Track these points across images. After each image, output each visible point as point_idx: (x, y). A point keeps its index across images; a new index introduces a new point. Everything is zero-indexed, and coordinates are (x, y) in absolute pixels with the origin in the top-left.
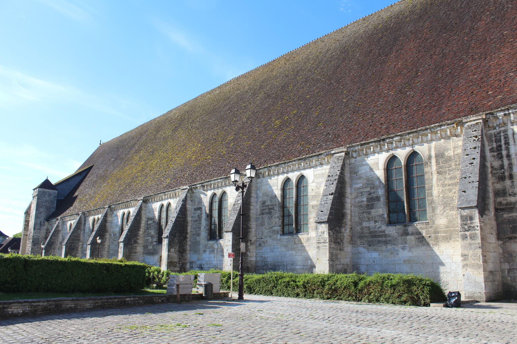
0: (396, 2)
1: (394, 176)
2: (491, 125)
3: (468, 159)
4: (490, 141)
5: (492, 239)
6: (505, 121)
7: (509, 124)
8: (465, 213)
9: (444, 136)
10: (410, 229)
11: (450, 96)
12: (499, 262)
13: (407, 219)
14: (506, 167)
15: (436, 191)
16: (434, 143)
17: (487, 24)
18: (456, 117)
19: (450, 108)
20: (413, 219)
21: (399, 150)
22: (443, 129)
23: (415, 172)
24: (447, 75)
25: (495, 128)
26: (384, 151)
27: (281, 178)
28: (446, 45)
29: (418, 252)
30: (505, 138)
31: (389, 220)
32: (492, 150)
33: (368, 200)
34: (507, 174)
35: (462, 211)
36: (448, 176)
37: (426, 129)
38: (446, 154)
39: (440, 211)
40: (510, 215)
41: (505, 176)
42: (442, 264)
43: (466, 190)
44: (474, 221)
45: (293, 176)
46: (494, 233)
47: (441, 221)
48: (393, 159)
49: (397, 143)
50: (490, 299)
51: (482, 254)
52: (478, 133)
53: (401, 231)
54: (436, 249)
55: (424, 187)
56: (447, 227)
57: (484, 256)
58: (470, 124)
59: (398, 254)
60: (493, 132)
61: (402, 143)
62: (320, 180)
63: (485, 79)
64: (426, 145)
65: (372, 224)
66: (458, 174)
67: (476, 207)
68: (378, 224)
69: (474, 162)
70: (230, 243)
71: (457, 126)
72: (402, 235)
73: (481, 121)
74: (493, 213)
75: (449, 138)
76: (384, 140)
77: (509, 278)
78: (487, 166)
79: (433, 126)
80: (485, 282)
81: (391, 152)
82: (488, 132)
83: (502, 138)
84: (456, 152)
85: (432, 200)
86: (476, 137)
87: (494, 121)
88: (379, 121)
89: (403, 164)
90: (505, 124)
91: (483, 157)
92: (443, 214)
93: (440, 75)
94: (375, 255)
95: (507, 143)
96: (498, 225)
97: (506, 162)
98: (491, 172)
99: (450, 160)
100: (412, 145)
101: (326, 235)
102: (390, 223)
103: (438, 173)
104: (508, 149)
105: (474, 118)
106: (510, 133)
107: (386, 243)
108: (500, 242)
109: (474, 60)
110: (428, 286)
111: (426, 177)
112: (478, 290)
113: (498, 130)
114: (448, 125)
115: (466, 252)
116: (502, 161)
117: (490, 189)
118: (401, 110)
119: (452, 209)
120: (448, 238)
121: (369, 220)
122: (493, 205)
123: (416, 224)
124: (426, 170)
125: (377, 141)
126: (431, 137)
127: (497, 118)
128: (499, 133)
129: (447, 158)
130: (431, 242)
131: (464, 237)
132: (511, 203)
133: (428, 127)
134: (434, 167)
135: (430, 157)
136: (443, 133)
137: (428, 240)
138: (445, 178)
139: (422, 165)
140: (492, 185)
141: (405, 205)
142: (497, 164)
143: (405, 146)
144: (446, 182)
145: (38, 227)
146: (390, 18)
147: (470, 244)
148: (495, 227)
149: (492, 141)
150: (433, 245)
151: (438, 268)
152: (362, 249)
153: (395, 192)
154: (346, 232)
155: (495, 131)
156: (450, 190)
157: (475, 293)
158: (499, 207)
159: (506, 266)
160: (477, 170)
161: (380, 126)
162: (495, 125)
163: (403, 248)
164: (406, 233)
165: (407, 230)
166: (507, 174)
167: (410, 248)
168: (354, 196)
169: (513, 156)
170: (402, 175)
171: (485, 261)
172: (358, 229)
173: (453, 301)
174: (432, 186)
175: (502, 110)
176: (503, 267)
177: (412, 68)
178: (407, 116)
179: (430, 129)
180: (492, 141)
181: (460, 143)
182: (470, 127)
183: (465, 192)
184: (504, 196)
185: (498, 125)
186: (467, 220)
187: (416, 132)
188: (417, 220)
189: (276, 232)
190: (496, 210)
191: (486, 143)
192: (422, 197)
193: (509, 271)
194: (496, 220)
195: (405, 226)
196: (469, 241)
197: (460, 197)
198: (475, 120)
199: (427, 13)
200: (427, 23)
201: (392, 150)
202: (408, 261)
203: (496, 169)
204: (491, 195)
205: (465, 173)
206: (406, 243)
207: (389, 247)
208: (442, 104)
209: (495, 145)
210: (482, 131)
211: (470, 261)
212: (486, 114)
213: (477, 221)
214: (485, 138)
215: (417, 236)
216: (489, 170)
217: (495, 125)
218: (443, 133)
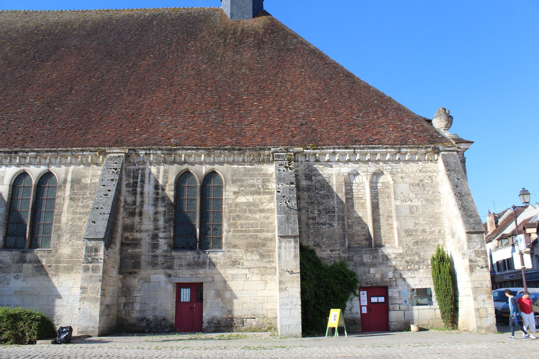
0: (68, 10)
1: (21, 194)
2: (132, 161)
3: (104, 190)
4: (128, 176)
5: (114, 273)
6: (145, 160)
7: (148, 164)
8: (91, 244)
9: (84, 162)
10: (29, 256)
11: (99, 122)
12: (117, 296)
13: (27, 244)
14: (137, 204)
15: (65, 218)
16: (72, 168)
17: (149, 65)
18: (101, 145)
19: (96, 135)
20: (34, 244)
21: (32, 167)
22: (84, 155)
23: (45, 193)
24: (101, 102)
25: (134, 165)
26: (14, 165)
28: (107, 72)
29: (34, 283)
30: (142, 176)
31: (5, 244)
32: (128, 185)
34: (137, 210)
35: (88, 242)
36: (80, 204)
37: (67, 151)
38: (83, 181)
39: (66, 239)
40: (134, 251)
41: (135, 213)
42: (59, 297)
43: (96, 221)
44: (98, 253)
46: (117, 267)
47: (65, 250)
48: (23, 175)
49: (32, 159)
50: (102, 334)
51: (102, 288)
52: (118, 166)
53: (16, 258)
54: (54, 280)
55: (53, 212)
56: (71, 257)
57: (103, 289)
58: (112, 155)
59: (8, 284)
60: (132, 167)
61: (38, 160)
63: (136, 116)
64: (63, 167)
66: (91, 203)
67: (103, 239)
69: (109, 194)
71: (100, 154)
72: (17, 262)
73: (123, 155)
74: (118, 247)
75: (89, 165)
76: (16, 152)
77: (124, 312)
78: (120, 201)
79: (75, 149)
80: (100, 316)
81: (22, 168)
82: (128, 167)
83: (140, 175)
84: (93, 181)
85: (60, 227)
86: (116, 169)
87: (135, 158)
88: (15, 130)
89: (34, 182)
90: (144, 163)
91: (118, 191)
92: (68, 243)
93: (94, 100)
95: (143, 181)
96: (121, 259)
97: (139, 199)
98: (124, 207)
99: (86, 188)
100: (48, 165)
103: (71, 199)
104: (142, 187)
105: (118, 151)
106: (147, 172)
108: (121, 277)
109: (130, 94)
110: (37, 320)
111: (57, 201)
112: (92, 324)
113: (137, 166)
114: (91, 152)
115: (85, 285)
116: (136, 198)
117: (120, 223)
118: (44, 124)
119: (79, 239)
120: (69, 269)
122: (120, 239)
123: (36, 251)
124: (59, 193)
125: (8, 152)
126: (71, 160)
127: (138, 155)
128: (138, 170)
129: (82, 185)
130: (50, 272)
131: (86, 269)
132: (136, 239)
133: (69, 149)
134: (68, 193)
135: (65, 181)
136: (84, 159)
137: (47, 269)
138: (77, 206)
139: (55, 187)
140: (122, 219)
141: (28, 228)
142: (130, 199)
143: (40, 164)
144: (77, 210)
146: (57, 24)
147: (91, 277)
148: (118, 262)
149: (130, 177)
150: (52, 275)
151: (54, 301)
153: (18, 213)
155: (134, 167)
156: (80, 219)
157: (88, 327)
158: (125, 242)
159: (123, 300)
160: (110, 202)
161: (15, 136)
162: (135, 161)
164: (23, 261)
165: (25, 257)
166: (137, 210)
167: (25, 277)
169: (146, 195)
170: (30, 195)
171: (103, 295)
173: (63, 336)
174: (62, 212)
175: (144, 149)
176: (120, 301)
177: (67, 84)
178: (49, 132)
179: (72, 151)
180: (130, 177)
181: (99, 173)
182: (111, 158)
183: (94, 222)
184: (131, 232)
185: (138, 163)
186: (91, 251)
187: (55, 151)
188: (37, 247)
190: (122, 244)
191: (124, 177)
192: (49, 222)
193: (125, 305)
194: (120, 254)
195: (23, 252)
196: (90, 273)
197: (89, 227)
198: (118, 152)
199: (97, 34)
200: (95, 43)
201: (24, 165)
202: (20, 293)
203: (128, 204)
204: (120, 229)
205: (98, 203)
206: (21, 271)
208: (90, 128)
209: (131, 181)
210: (122, 165)
211: (89, 294)
212: (129, 149)
213: (101, 254)
214: (124, 172)
215: (35, 265)
216: (122, 204)
217: (135, 161)
218: (84, 159)
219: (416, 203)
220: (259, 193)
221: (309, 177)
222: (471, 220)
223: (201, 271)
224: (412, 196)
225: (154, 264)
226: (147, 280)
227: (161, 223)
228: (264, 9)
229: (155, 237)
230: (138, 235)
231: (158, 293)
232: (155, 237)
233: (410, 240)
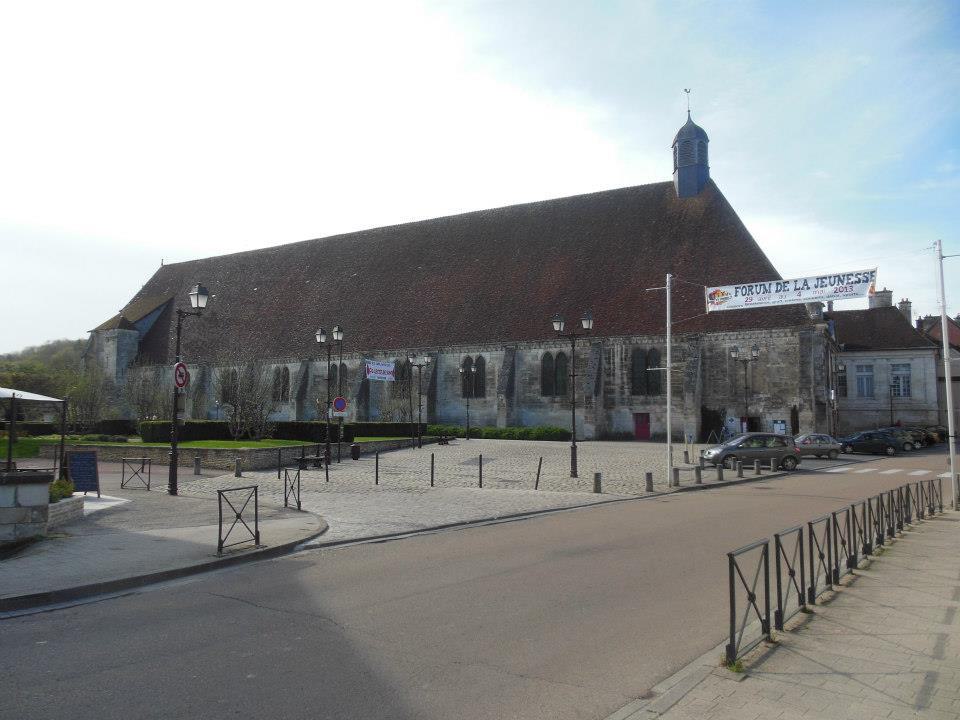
27: (463, 355)
33: (530, 380)
65: (532, 394)
90: (613, 344)
94: (533, 414)
95: (614, 356)
101: (504, 402)
102: (545, 393)
107: (540, 407)
140: (604, 378)
142: (607, 367)
145: (120, 375)
152: (524, 410)
154: (515, 398)
172: (522, 397)
189: (459, 396)
204: (603, 384)
207: (542, 410)
219: (783, 365)
220: (680, 361)
221: (711, 350)
222: (804, 380)
223: (648, 407)
224: (780, 360)
225: (623, 404)
226: (619, 412)
227: (625, 380)
228: (714, 175)
229: (622, 388)
231: (625, 418)
232: (622, 388)
233: (776, 390)
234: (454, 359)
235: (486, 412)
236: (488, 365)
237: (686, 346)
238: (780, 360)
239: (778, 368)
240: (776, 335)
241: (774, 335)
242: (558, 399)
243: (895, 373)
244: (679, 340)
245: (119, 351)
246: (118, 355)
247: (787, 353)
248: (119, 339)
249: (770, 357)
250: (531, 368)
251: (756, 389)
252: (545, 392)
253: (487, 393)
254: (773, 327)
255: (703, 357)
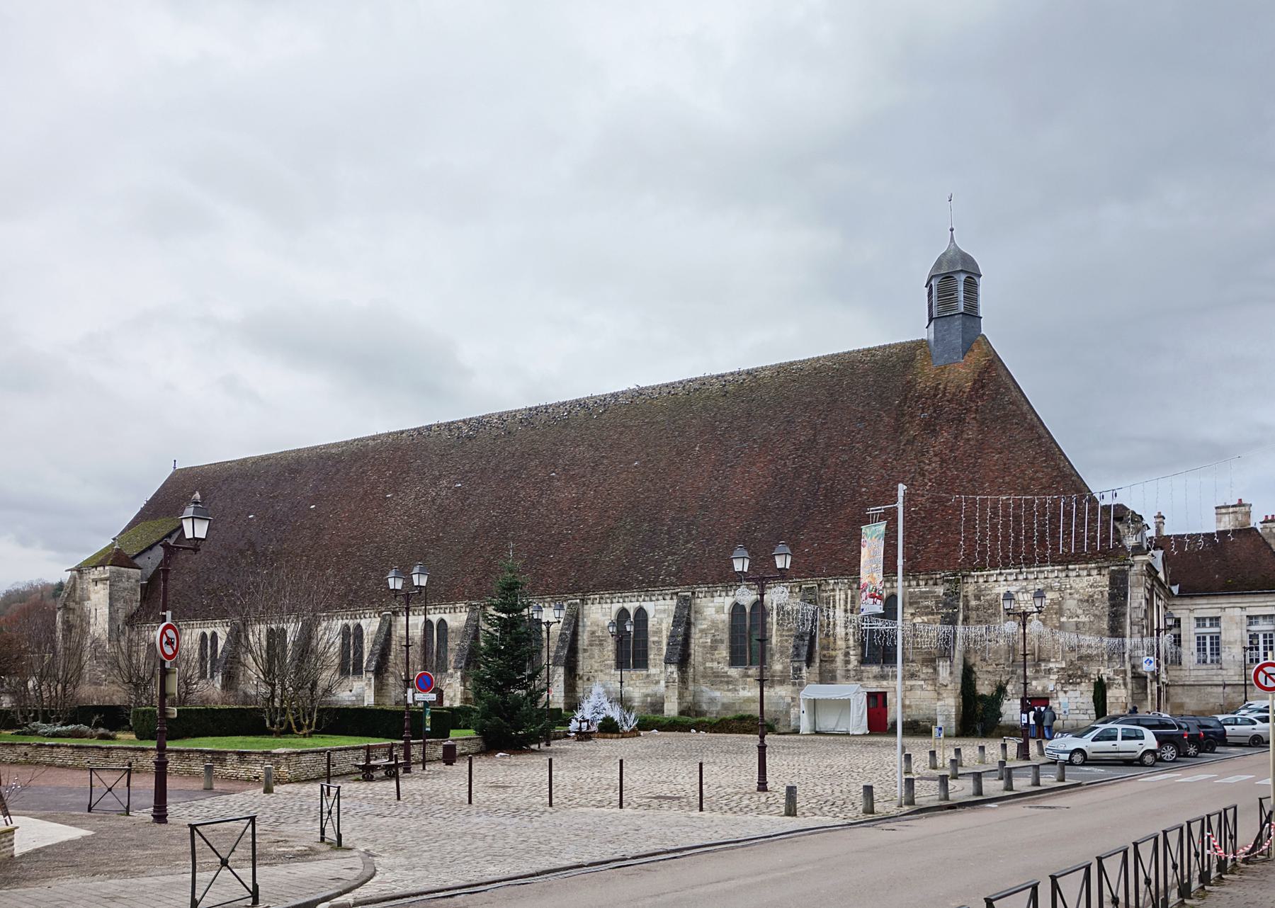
15: (774, 640)
27: (616, 607)
45: (631, 607)
47: (778, 667)
62: (662, 616)
65: (715, 665)
68: (721, 666)
70: (562, 678)
89: (748, 610)
90: (833, 590)
101: (675, 675)
107: (728, 683)
121: (712, 660)
163: (744, 689)
168: (697, 636)
219: (1083, 619)
221: (978, 598)
223: (885, 683)
224: (1079, 612)
227: (851, 642)
229: (847, 654)
230: (833, 653)
234: (600, 614)
235: (649, 691)
236: (652, 622)
237: (940, 590)
238: (1079, 612)
239: (1077, 624)
240: (1074, 574)
241: (1073, 574)
242: (753, 671)
243: (1253, 628)
244: (931, 582)
245: (112, 599)
246: (111, 605)
247: (1090, 600)
248: (113, 582)
249: (1065, 607)
250: (714, 624)
251: (1044, 656)
252: (735, 660)
253: (651, 662)
254: (1070, 563)
255: (967, 607)
